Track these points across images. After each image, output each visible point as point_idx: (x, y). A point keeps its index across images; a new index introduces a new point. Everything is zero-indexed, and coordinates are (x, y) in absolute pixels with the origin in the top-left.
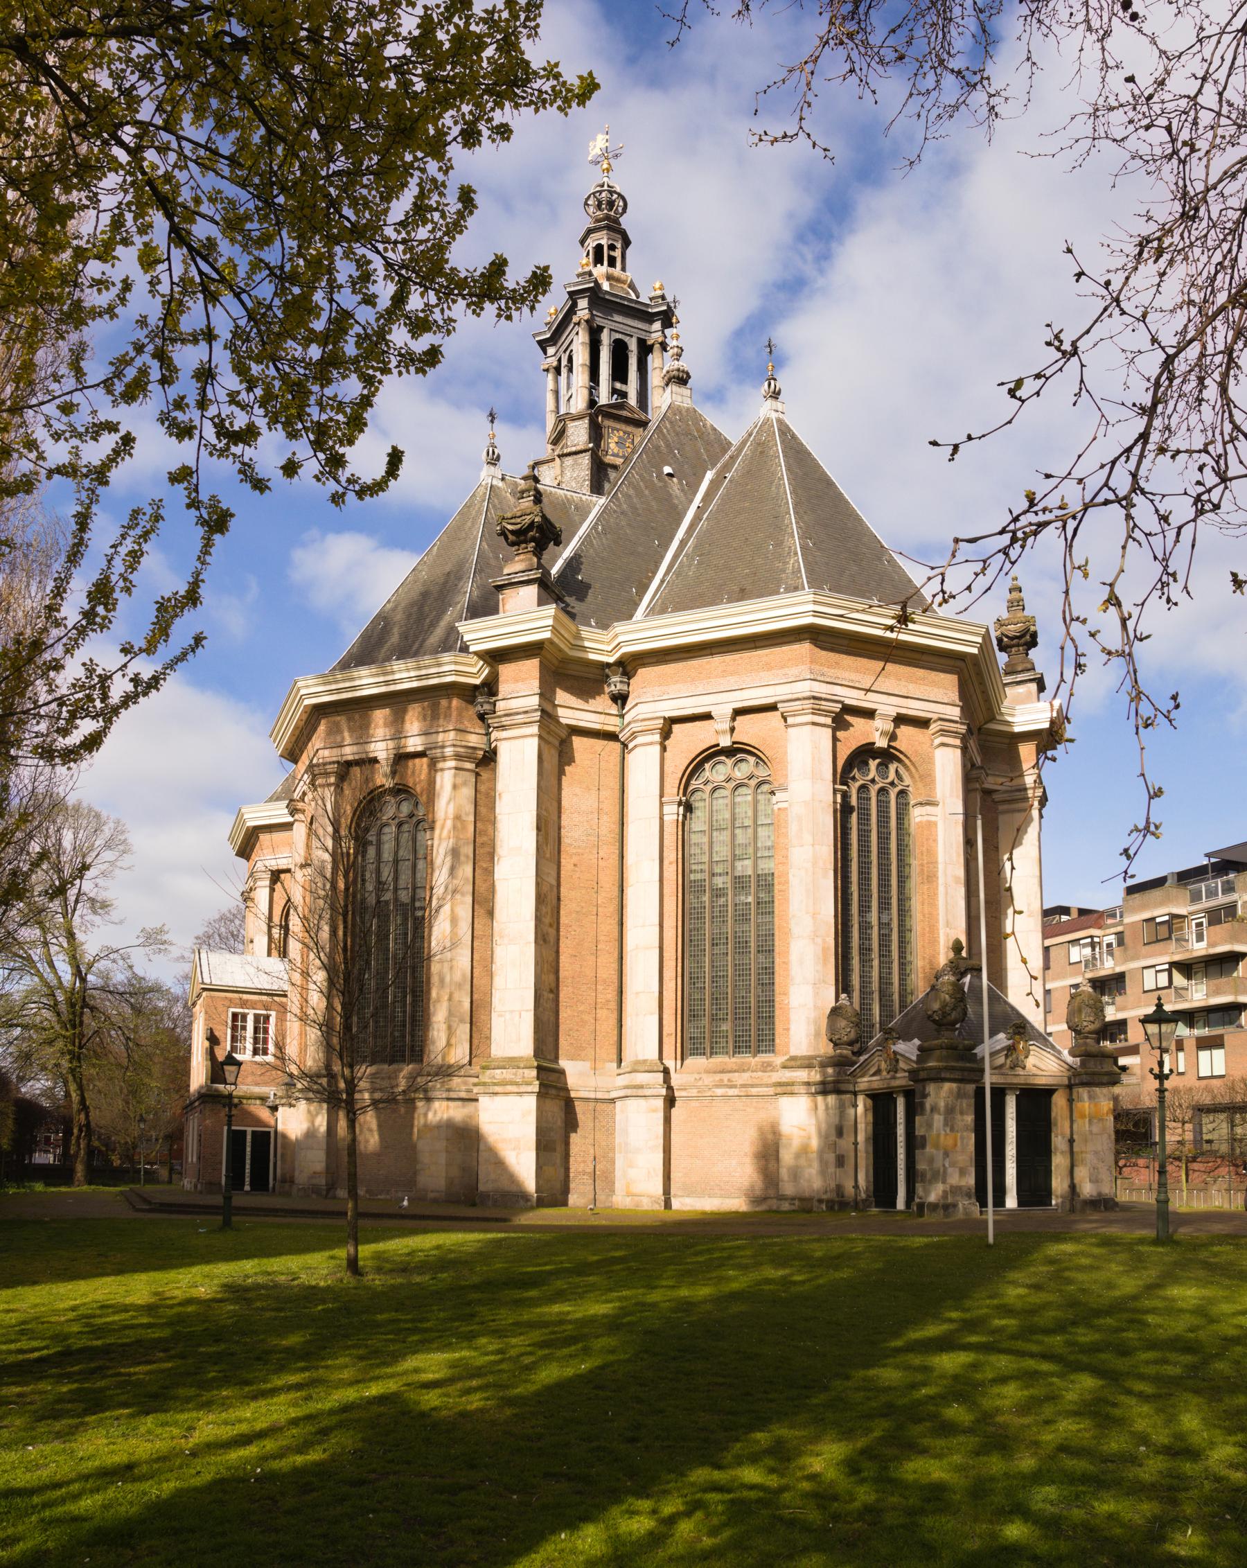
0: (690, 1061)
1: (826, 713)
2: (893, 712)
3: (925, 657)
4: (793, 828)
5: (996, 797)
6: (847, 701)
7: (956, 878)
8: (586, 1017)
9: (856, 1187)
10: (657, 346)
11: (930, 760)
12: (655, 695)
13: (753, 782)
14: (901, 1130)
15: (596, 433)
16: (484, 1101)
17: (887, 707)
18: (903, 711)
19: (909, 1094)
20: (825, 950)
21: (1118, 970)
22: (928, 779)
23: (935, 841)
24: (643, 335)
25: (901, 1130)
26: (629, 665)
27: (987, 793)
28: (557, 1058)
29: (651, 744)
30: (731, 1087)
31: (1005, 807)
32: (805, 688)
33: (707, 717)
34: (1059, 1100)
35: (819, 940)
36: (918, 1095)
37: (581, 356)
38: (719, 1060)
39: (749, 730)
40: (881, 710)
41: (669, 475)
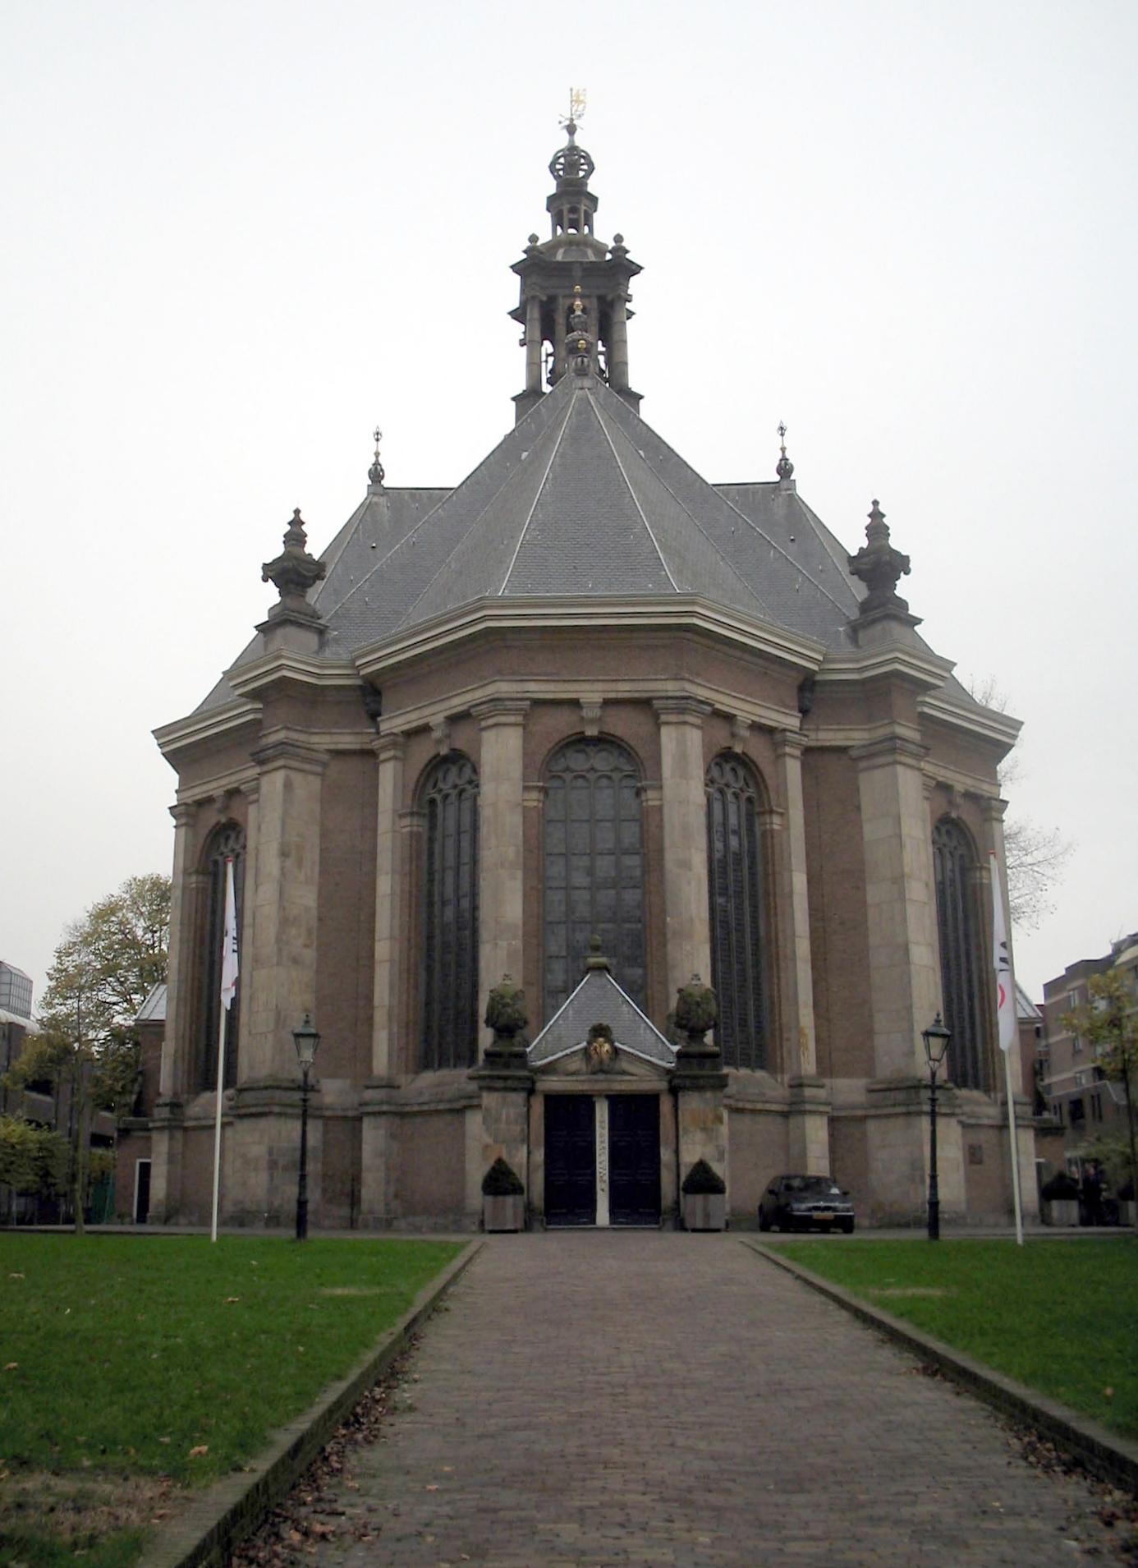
0: (429, 1078)
2: (598, 698)
3: (635, 635)
5: (854, 753)
17: (591, 693)
23: (661, 827)
24: (602, 292)
30: (441, 1101)
34: (665, 1105)
40: (584, 698)
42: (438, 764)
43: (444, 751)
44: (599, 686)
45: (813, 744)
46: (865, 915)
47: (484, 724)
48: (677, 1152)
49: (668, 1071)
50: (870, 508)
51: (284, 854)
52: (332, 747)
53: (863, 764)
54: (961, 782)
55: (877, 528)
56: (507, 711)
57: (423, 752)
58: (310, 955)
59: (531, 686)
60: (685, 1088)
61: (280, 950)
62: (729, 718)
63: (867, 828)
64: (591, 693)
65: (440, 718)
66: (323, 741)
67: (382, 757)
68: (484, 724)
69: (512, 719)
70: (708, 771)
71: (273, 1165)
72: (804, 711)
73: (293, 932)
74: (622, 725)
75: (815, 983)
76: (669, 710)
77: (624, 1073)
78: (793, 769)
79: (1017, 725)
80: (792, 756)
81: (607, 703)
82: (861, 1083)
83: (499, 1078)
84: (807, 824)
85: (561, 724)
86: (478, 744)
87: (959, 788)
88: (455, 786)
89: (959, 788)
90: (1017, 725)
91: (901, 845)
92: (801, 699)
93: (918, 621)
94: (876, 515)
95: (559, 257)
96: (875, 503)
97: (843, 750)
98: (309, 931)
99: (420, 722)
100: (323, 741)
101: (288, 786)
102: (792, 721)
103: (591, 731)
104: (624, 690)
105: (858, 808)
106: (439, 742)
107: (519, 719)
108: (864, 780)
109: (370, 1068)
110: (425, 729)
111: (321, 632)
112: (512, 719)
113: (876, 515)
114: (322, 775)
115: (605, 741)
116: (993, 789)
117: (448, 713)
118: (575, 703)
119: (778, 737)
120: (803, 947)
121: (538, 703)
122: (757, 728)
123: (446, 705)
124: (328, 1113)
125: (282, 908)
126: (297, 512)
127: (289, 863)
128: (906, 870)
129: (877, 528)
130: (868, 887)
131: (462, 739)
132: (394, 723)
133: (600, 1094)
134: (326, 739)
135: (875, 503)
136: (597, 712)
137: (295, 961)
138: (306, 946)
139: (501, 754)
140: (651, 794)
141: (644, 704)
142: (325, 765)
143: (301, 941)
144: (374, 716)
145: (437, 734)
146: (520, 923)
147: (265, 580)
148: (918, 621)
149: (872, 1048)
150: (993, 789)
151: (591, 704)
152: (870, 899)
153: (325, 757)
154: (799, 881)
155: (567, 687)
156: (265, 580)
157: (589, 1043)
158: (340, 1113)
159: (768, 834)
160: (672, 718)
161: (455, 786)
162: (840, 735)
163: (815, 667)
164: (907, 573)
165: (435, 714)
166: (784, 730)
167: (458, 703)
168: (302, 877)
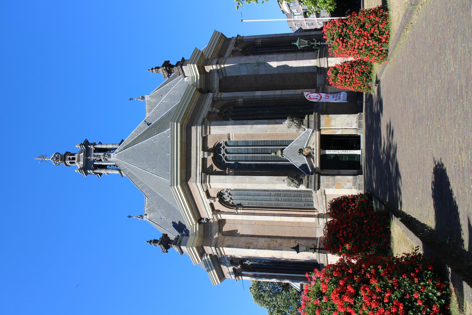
0: (315, 206)
1: (206, 177)
6: (201, 171)
7: (251, 128)
10: (95, 146)
11: (215, 136)
12: (206, 213)
13: (230, 196)
17: (201, 154)
20: (278, 180)
22: (221, 136)
23: (240, 134)
24: (93, 151)
26: (199, 219)
28: (315, 239)
32: (199, 184)
34: (323, 132)
35: (275, 182)
38: (314, 200)
42: (222, 201)
43: (217, 199)
45: (218, 89)
46: (269, 74)
48: (338, 129)
51: (249, 248)
53: (224, 75)
54: (231, 47)
57: (218, 206)
61: (277, 250)
62: (209, 113)
63: (243, 74)
65: (208, 200)
67: (220, 218)
70: (225, 120)
72: (208, 92)
73: (272, 245)
75: (289, 89)
78: (225, 95)
79: (216, 32)
80: (221, 95)
82: (318, 76)
84: (242, 91)
86: (215, 189)
87: (234, 48)
88: (228, 196)
89: (234, 48)
90: (216, 32)
91: (248, 63)
92: (205, 93)
93: (183, 58)
95: (82, 163)
97: (220, 80)
98: (272, 241)
101: (228, 246)
102: (211, 95)
104: (200, 144)
105: (237, 76)
106: (215, 201)
107: (208, 176)
108: (228, 75)
109: (314, 223)
110: (212, 205)
111: (183, 235)
116: (234, 39)
117: (206, 198)
119: (215, 99)
120: (278, 92)
122: (213, 105)
125: (265, 249)
126: (147, 242)
127: (252, 247)
128: (255, 62)
130: (261, 73)
133: (320, 152)
137: (281, 245)
138: (276, 242)
143: (275, 243)
145: (212, 201)
146: (269, 177)
147: (167, 252)
148: (183, 58)
149: (308, 73)
150: (234, 39)
151: (204, 155)
152: (265, 73)
154: (258, 93)
156: (167, 252)
157: (304, 155)
159: (244, 102)
161: (228, 196)
162: (216, 81)
163: (195, 88)
164: (169, 62)
166: (213, 97)
167: (204, 195)
168: (256, 243)
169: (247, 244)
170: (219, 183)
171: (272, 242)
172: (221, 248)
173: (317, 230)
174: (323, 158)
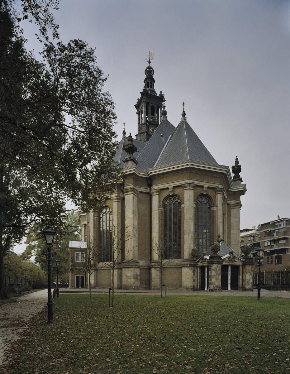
2: (207, 186)
4: (185, 211)
6: (197, 184)
8: (144, 251)
9: (197, 286)
11: (215, 197)
14: (206, 274)
15: (148, 127)
16: (123, 269)
18: (209, 186)
19: (208, 266)
21: (258, 242)
22: (216, 201)
23: (216, 214)
24: (158, 104)
25: (206, 274)
27: (228, 204)
29: (156, 195)
31: (232, 207)
32: (187, 181)
33: (168, 188)
34: (241, 268)
36: (209, 267)
37: (144, 110)
39: (177, 191)
40: (205, 186)
41: (162, 136)
42: (169, 197)
43: (171, 194)
44: (207, 184)
47: (185, 189)
49: (243, 261)
50: (236, 158)
52: (140, 191)
55: (237, 162)
56: (191, 186)
57: (166, 193)
58: (137, 235)
59: (195, 182)
60: (246, 265)
64: (206, 185)
65: (172, 186)
66: (139, 189)
68: (185, 189)
69: (192, 188)
71: (134, 278)
74: (210, 193)
76: (219, 191)
77: (235, 261)
81: (209, 188)
83: (217, 261)
85: (199, 190)
86: (184, 192)
94: (237, 159)
96: (237, 157)
99: (166, 187)
100: (139, 189)
103: (205, 193)
106: (171, 192)
107: (193, 188)
112: (192, 188)
113: (237, 159)
114: (137, 197)
115: (207, 196)
118: (202, 187)
121: (197, 186)
123: (174, 183)
124: (141, 267)
129: (237, 162)
131: (177, 191)
132: (156, 187)
134: (139, 189)
135: (237, 157)
136: (206, 189)
139: (188, 197)
140: (215, 208)
141: (213, 189)
142: (138, 195)
144: (150, 186)
153: (138, 193)
155: (202, 183)
158: (143, 267)
160: (220, 193)
165: (171, 185)
167: (177, 183)
169: (135, 212)
170: (188, 197)
171: (136, 230)
172: (132, 192)
173: (144, 261)
174: (227, 267)
